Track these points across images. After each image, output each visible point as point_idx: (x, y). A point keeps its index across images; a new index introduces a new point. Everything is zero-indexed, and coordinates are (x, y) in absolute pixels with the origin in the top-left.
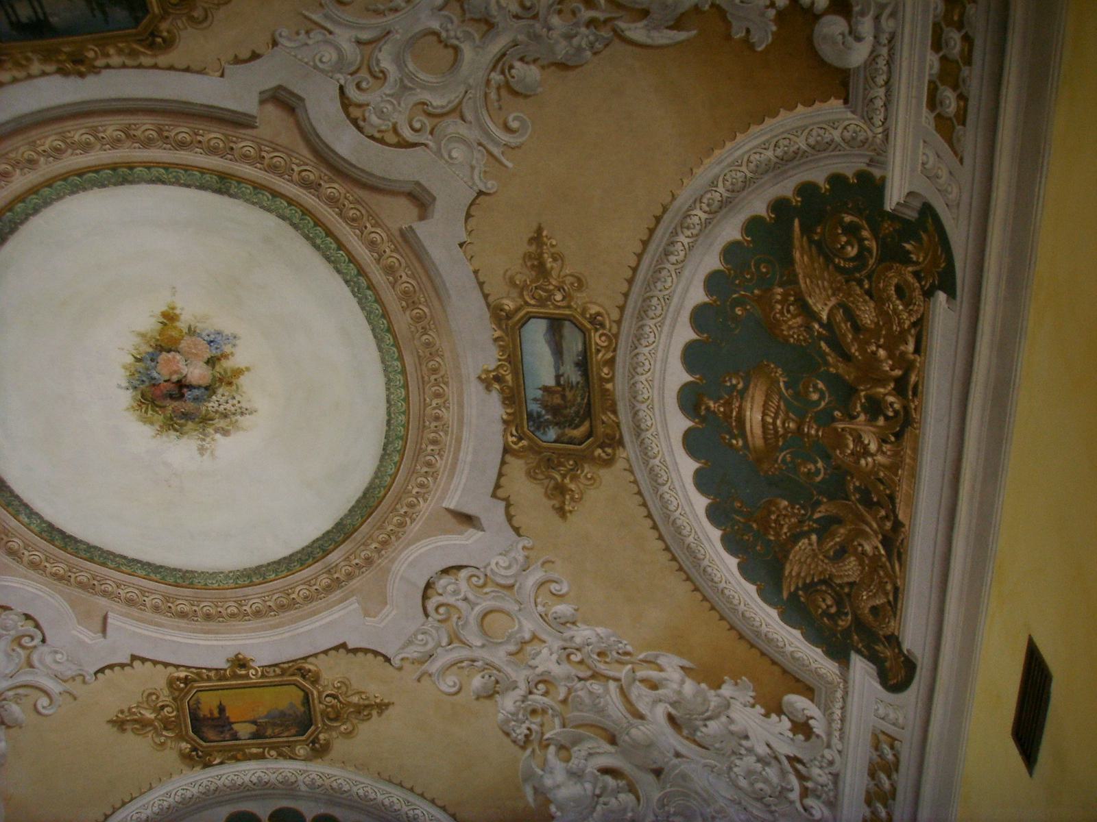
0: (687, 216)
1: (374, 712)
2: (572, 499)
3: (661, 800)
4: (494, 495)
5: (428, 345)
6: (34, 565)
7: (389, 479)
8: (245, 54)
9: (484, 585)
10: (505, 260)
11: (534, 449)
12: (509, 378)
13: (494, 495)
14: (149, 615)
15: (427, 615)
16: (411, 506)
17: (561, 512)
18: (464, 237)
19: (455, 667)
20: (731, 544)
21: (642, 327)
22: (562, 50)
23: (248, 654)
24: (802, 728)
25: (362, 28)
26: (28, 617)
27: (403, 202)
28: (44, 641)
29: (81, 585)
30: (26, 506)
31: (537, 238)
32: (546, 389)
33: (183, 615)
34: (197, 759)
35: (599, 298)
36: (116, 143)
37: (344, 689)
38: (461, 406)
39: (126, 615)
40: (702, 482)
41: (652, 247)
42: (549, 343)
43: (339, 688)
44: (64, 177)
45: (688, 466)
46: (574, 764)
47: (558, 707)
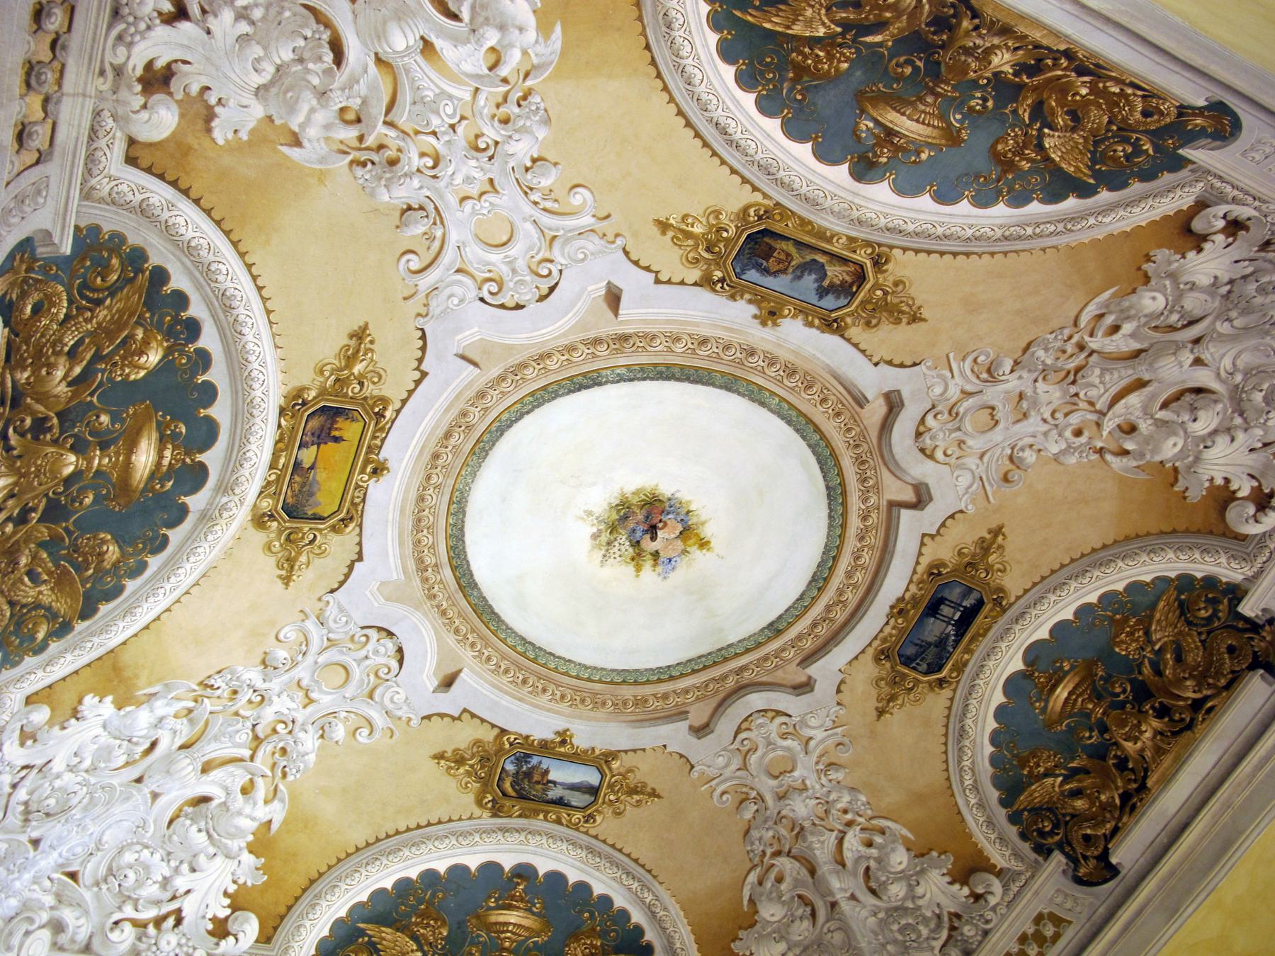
0: (649, 890)
1: (283, 573)
2: (450, 768)
3: (111, 786)
4: (465, 710)
5: (604, 704)
6: (571, 349)
7: (503, 636)
8: (842, 688)
9: (377, 675)
10: (646, 771)
11: (500, 751)
12: (562, 750)
13: (465, 710)
14: (461, 405)
15: (362, 628)
16: (473, 645)
17: (440, 757)
18: (669, 749)
19: (303, 639)
20: (404, 886)
21: (581, 848)
22: (755, 834)
23: (385, 479)
24: (221, 930)
25: (817, 745)
26: (519, 307)
27: (704, 720)
28: (482, 300)
29: (523, 366)
30: (631, 380)
31: (654, 794)
32: (547, 772)
33: (448, 435)
34: (294, 404)
35: (605, 823)
36: (840, 592)
37: (318, 551)
38: (549, 710)
39: (471, 384)
40: (459, 871)
41: (633, 864)
42: (581, 783)
43: (320, 547)
44: (839, 548)
45: (473, 862)
46: (171, 722)
47: (234, 709)
